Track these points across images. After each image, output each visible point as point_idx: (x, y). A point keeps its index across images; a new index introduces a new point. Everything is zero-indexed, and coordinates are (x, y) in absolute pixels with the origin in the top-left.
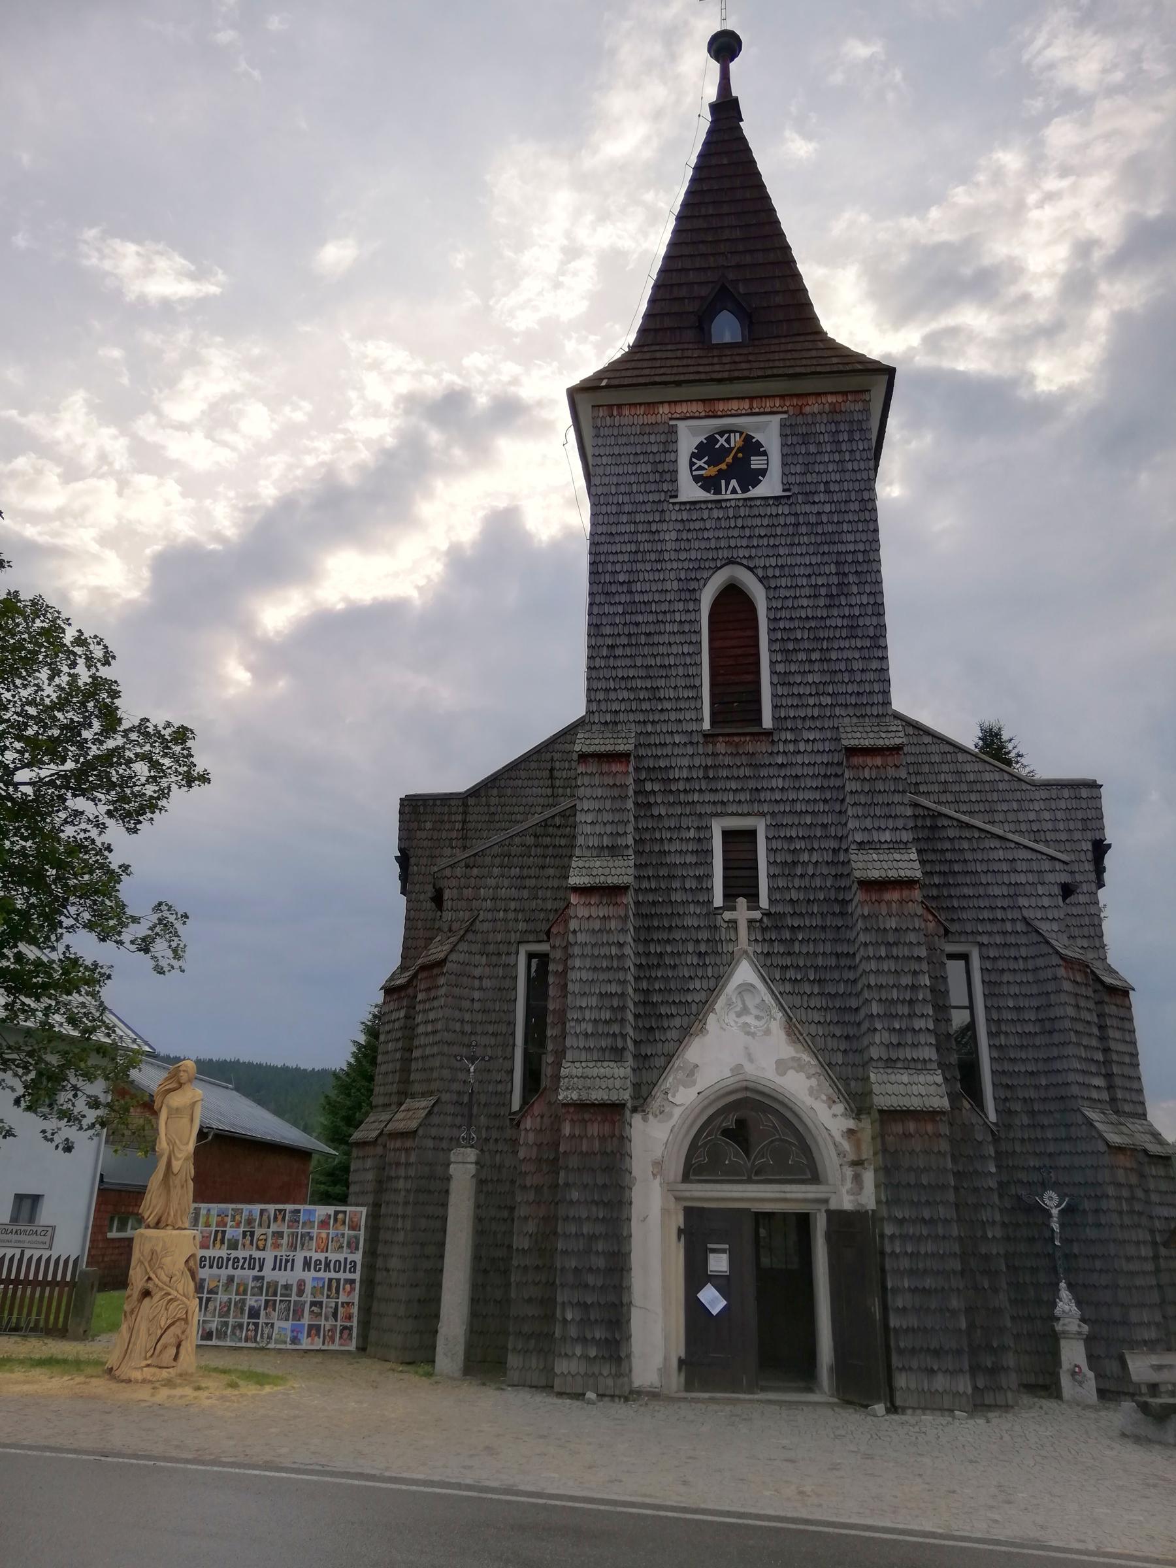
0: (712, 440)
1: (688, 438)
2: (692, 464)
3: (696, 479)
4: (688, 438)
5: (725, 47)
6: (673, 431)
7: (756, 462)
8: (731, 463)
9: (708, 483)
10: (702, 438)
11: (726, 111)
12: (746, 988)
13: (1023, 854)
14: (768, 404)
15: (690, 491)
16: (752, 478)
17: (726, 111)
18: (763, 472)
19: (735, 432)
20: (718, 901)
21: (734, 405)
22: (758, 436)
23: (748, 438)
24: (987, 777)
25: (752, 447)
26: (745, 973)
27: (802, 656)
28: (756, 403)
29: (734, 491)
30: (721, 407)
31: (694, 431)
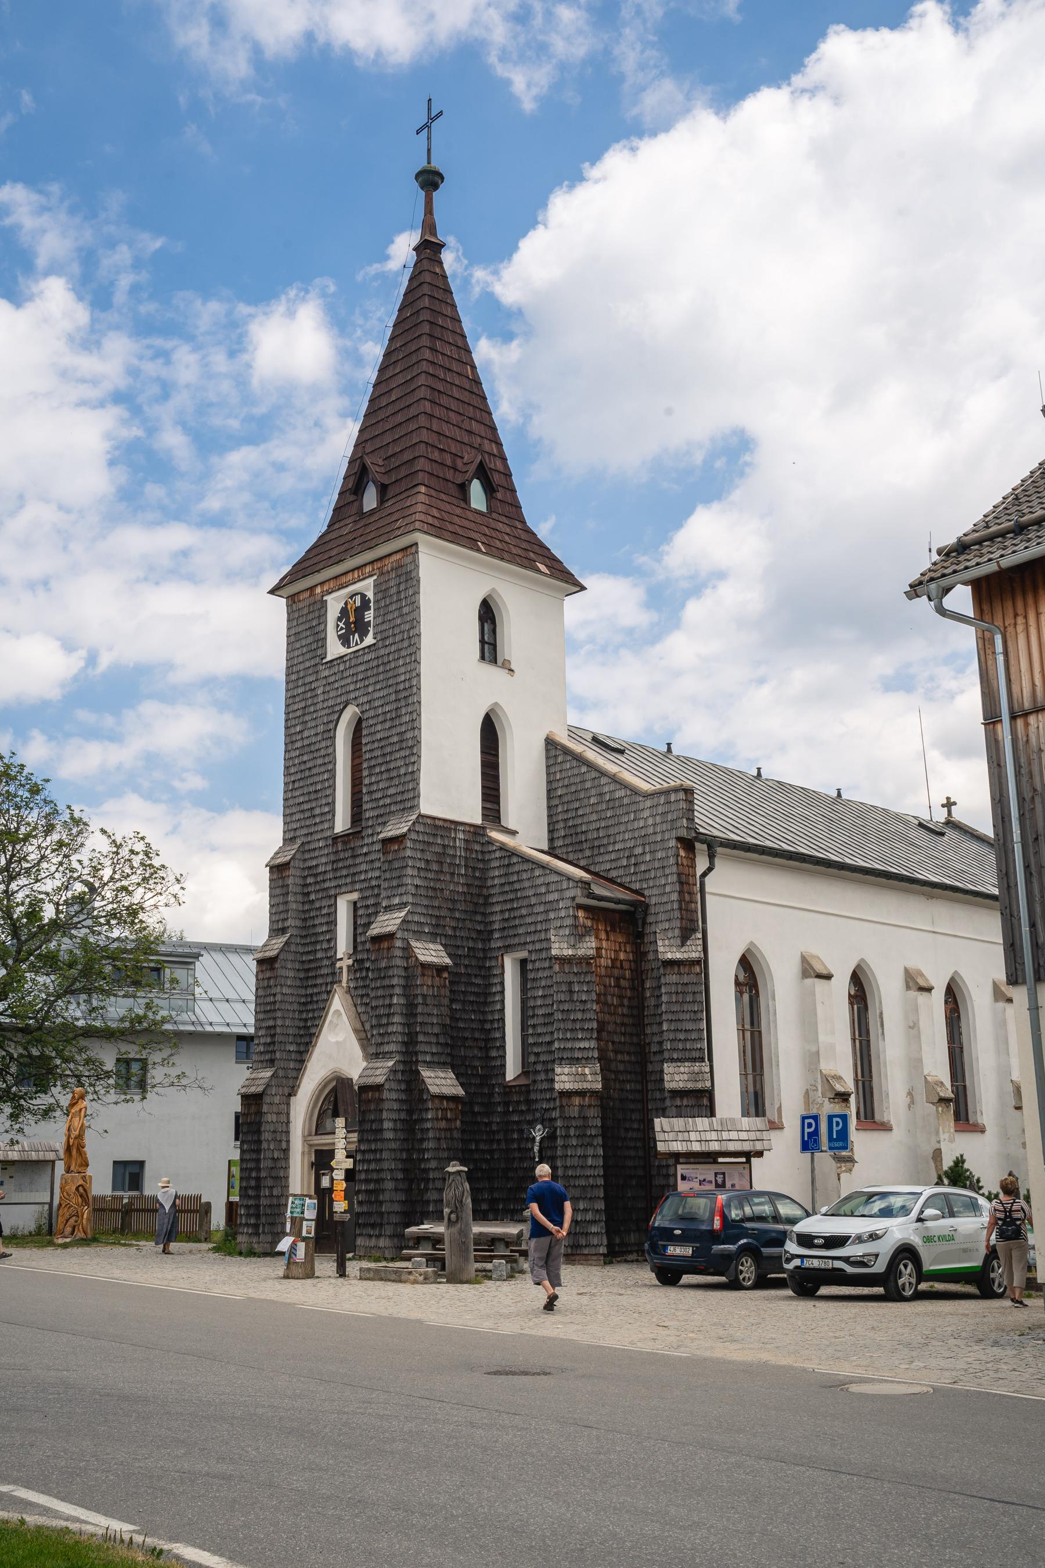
1: (334, 604)
2: (338, 626)
3: (340, 637)
4: (334, 604)
5: (430, 180)
6: (324, 604)
9: (345, 640)
10: (342, 605)
12: (337, 1011)
13: (554, 878)
14: (368, 569)
19: (357, 594)
21: (350, 576)
23: (363, 596)
24: (618, 794)
27: (377, 770)
29: (357, 644)
30: (344, 579)
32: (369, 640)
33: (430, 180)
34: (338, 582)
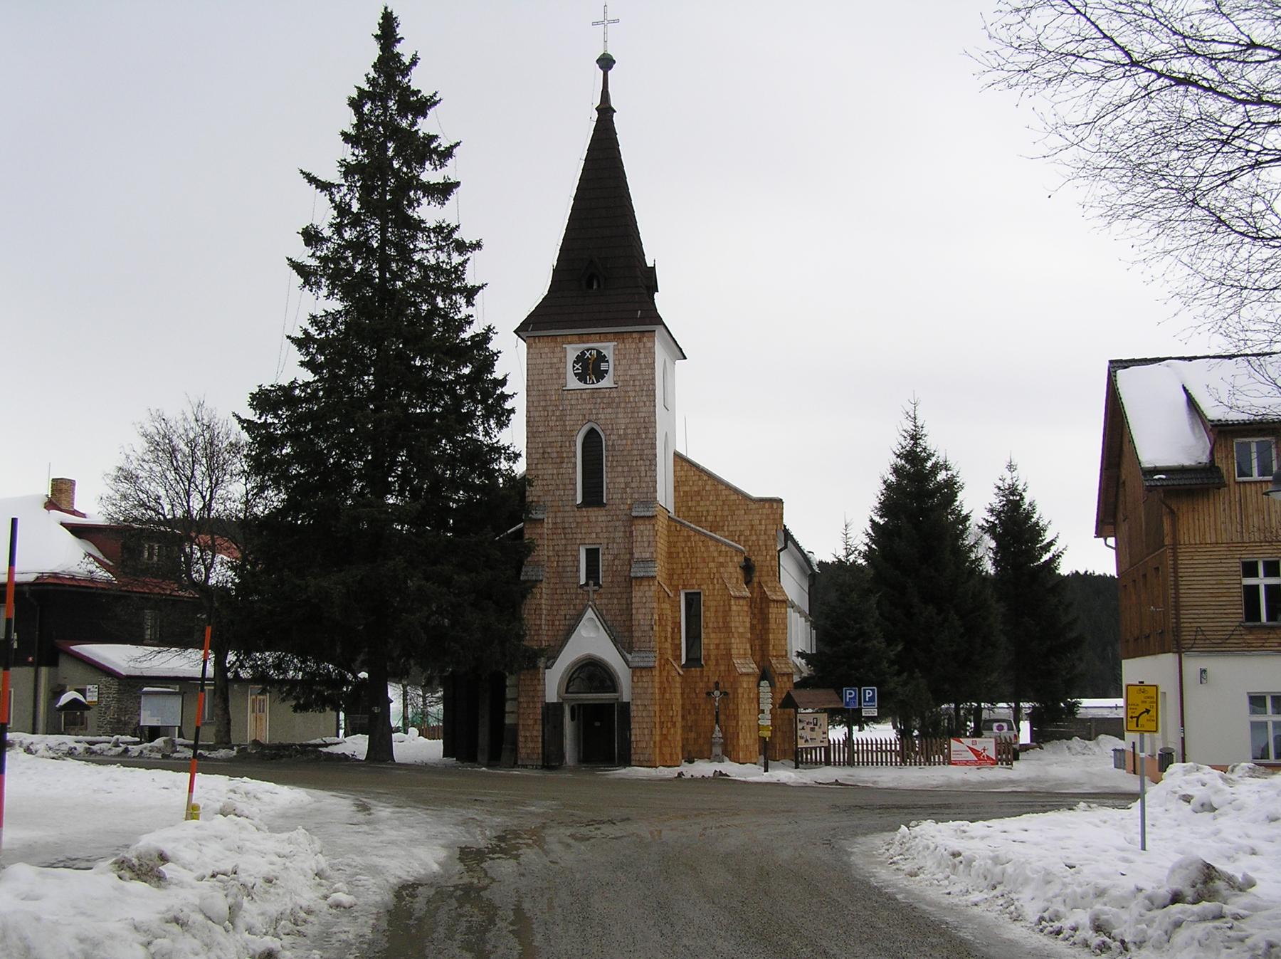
0: (583, 353)
4: (572, 351)
5: (606, 63)
7: (603, 366)
8: (591, 367)
9: (582, 377)
11: (605, 111)
15: (573, 383)
16: (600, 375)
17: (605, 111)
18: (606, 372)
20: (583, 581)
22: (604, 352)
23: (599, 352)
25: (601, 358)
26: (590, 613)
27: (620, 469)
28: (604, 337)
31: (576, 349)
32: (606, 383)
33: (606, 63)
34: (581, 338)
